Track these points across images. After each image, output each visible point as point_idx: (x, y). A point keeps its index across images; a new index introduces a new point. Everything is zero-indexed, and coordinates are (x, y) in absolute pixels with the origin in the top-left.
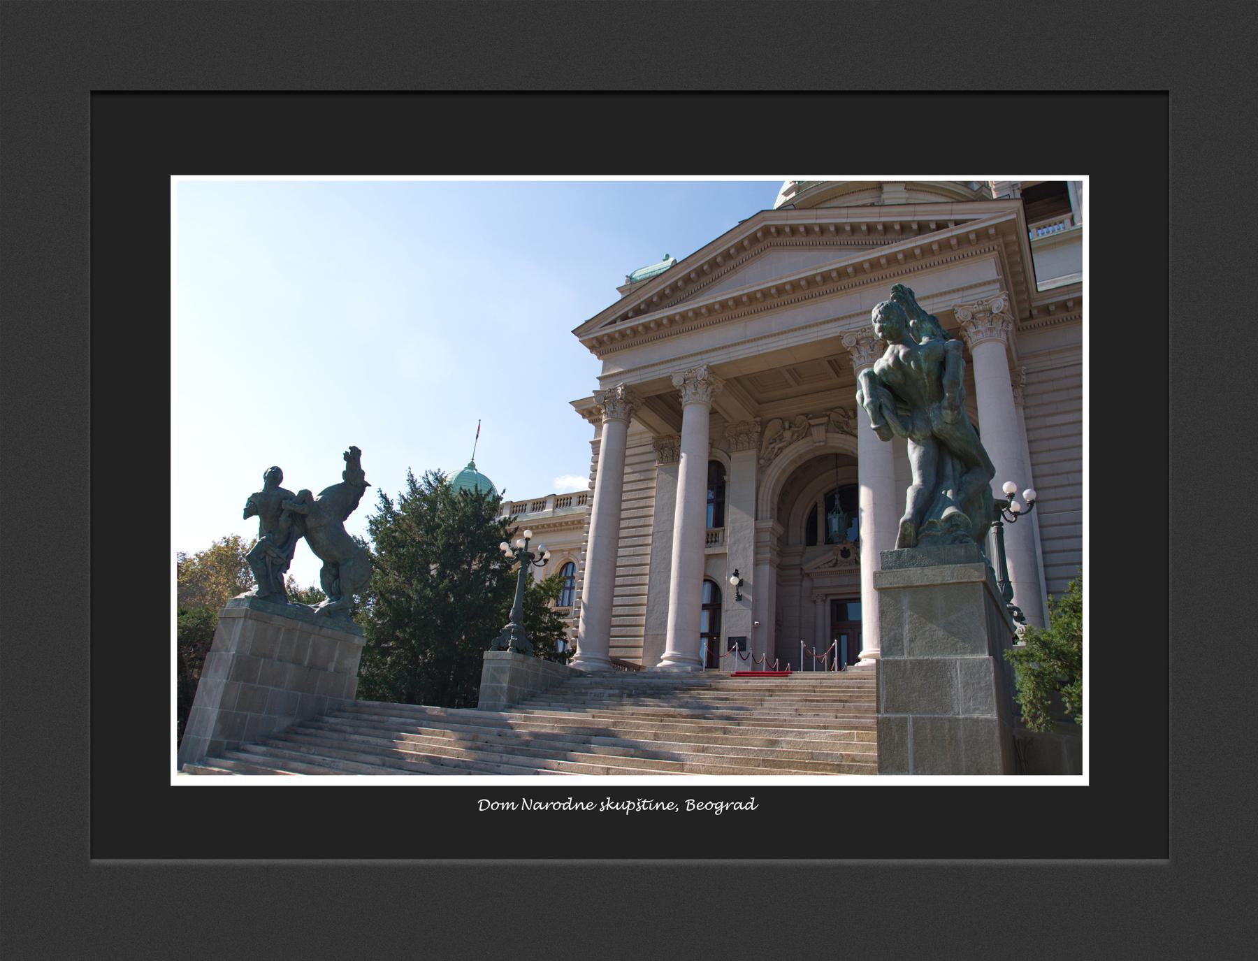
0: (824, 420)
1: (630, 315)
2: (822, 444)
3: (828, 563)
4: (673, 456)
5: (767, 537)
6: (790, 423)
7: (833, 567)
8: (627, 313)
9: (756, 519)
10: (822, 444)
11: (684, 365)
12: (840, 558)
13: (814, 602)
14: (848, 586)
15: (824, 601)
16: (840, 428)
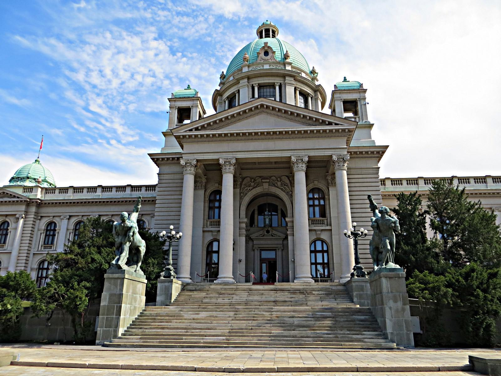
0: (268, 180)
1: (200, 128)
2: (267, 190)
3: (261, 235)
4: (201, 186)
5: (244, 225)
6: (254, 180)
7: (263, 236)
8: (198, 127)
9: (240, 218)
10: (267, 190)
11: (225, 155)
12: (266, 233)
13: (254, 250)
14: (268, 244)
15: (258, 250)
16: (274, 185)
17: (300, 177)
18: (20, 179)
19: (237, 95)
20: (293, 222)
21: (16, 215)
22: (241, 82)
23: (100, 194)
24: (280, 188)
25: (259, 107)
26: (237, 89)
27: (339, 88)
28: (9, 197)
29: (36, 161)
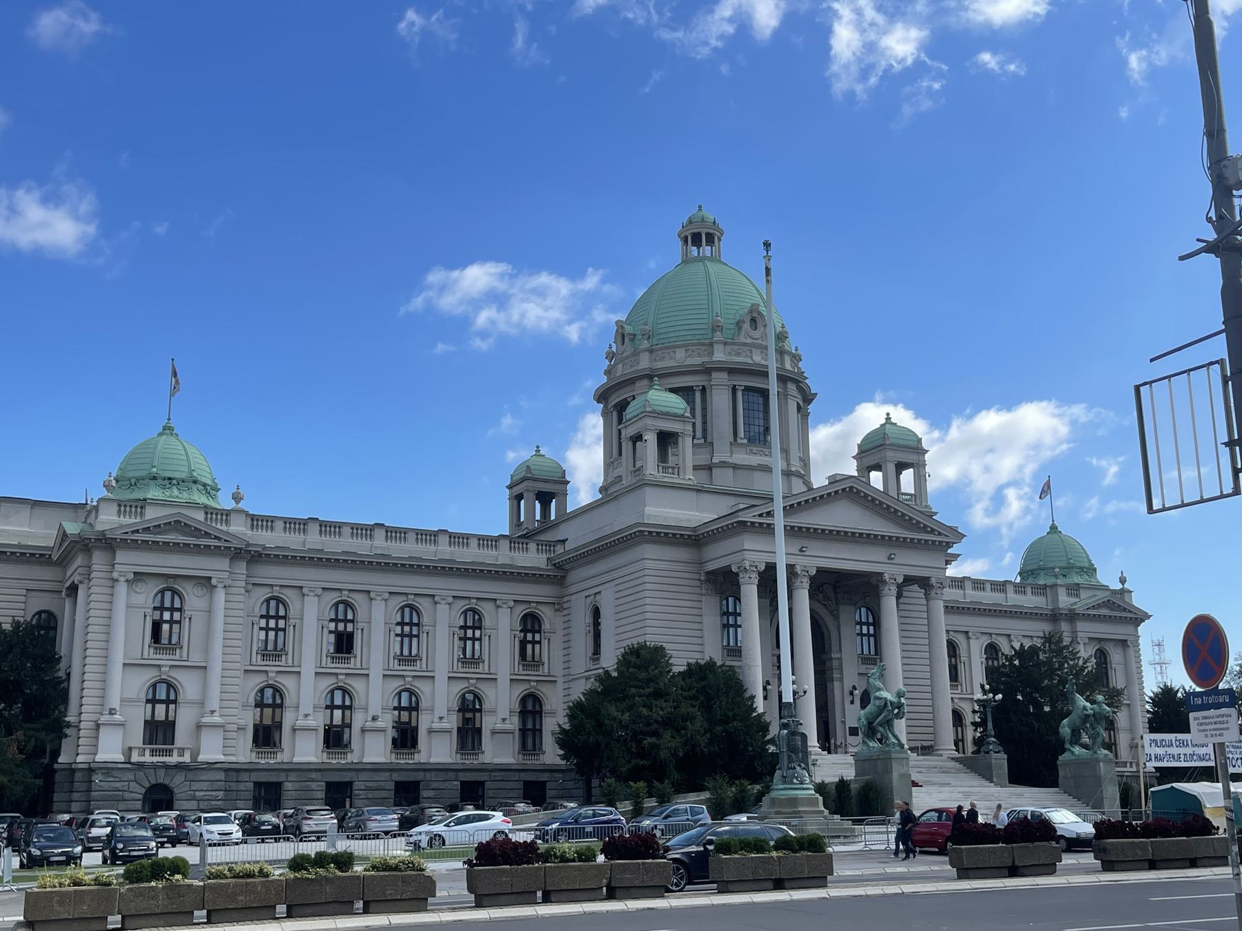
17: (889, 604)
18: (174, 482)
19: (698, 395)
20: (840, 659)
21: (210, 578)
22: (715, 375)
23: (385, 544)
24: (822, 604)
25: (847, 489)
26: (703, 383)
27: (892, 441)
28: (184, 534)
29: (165, 428)
